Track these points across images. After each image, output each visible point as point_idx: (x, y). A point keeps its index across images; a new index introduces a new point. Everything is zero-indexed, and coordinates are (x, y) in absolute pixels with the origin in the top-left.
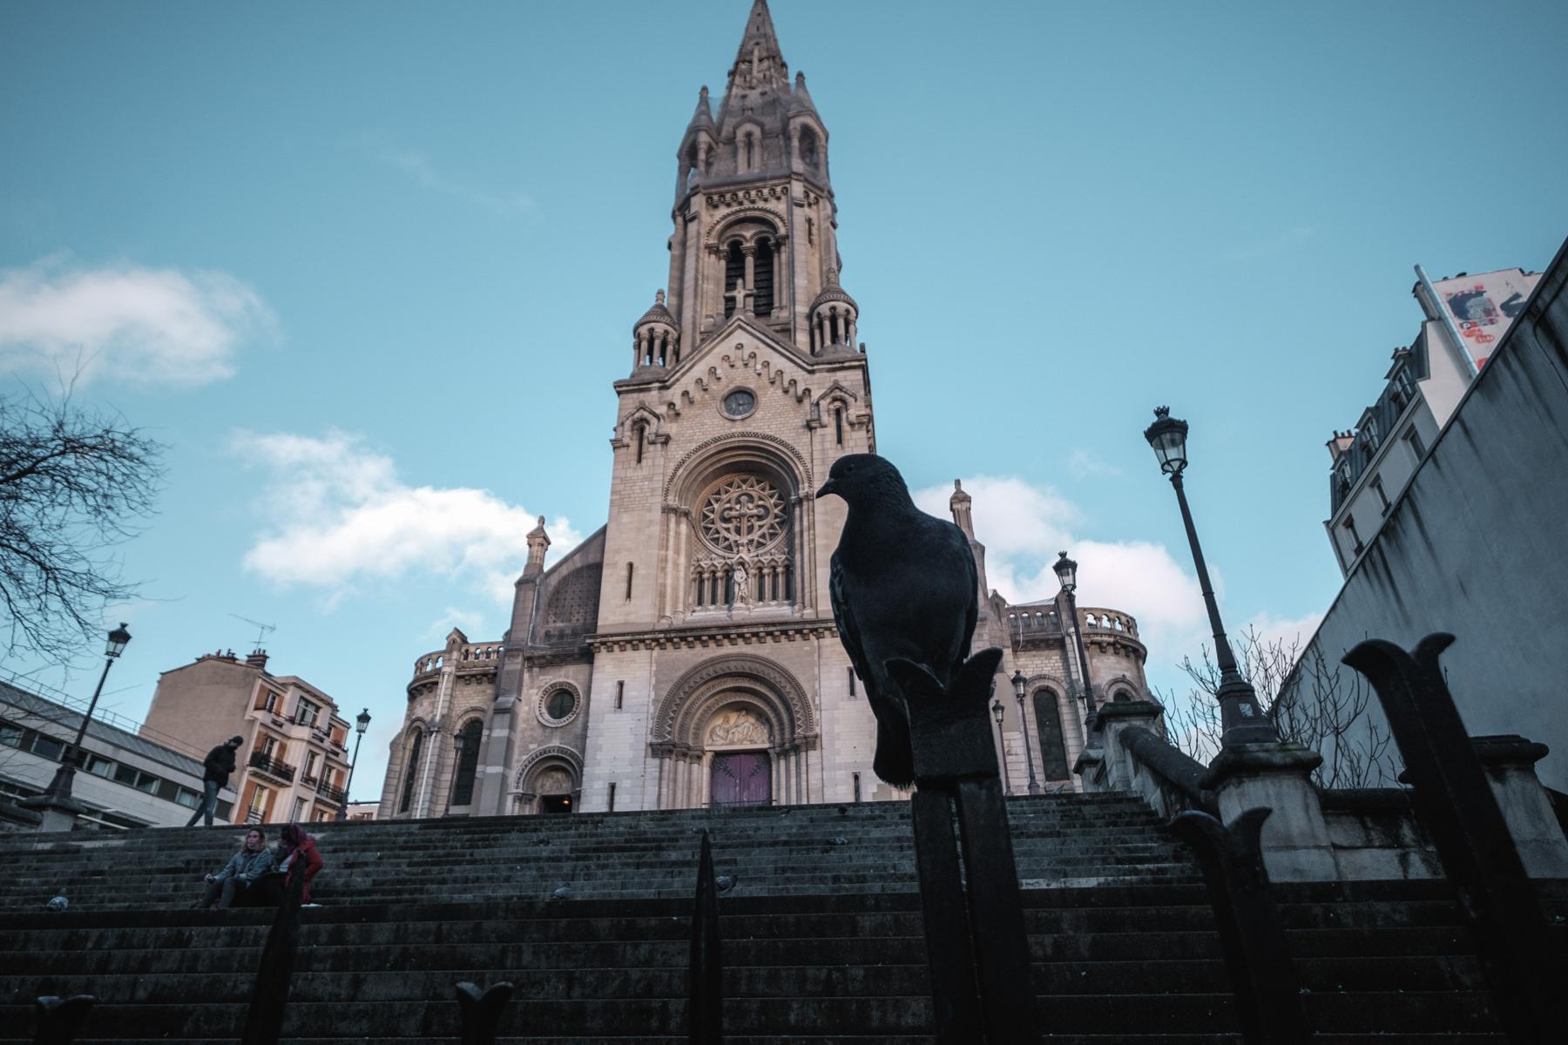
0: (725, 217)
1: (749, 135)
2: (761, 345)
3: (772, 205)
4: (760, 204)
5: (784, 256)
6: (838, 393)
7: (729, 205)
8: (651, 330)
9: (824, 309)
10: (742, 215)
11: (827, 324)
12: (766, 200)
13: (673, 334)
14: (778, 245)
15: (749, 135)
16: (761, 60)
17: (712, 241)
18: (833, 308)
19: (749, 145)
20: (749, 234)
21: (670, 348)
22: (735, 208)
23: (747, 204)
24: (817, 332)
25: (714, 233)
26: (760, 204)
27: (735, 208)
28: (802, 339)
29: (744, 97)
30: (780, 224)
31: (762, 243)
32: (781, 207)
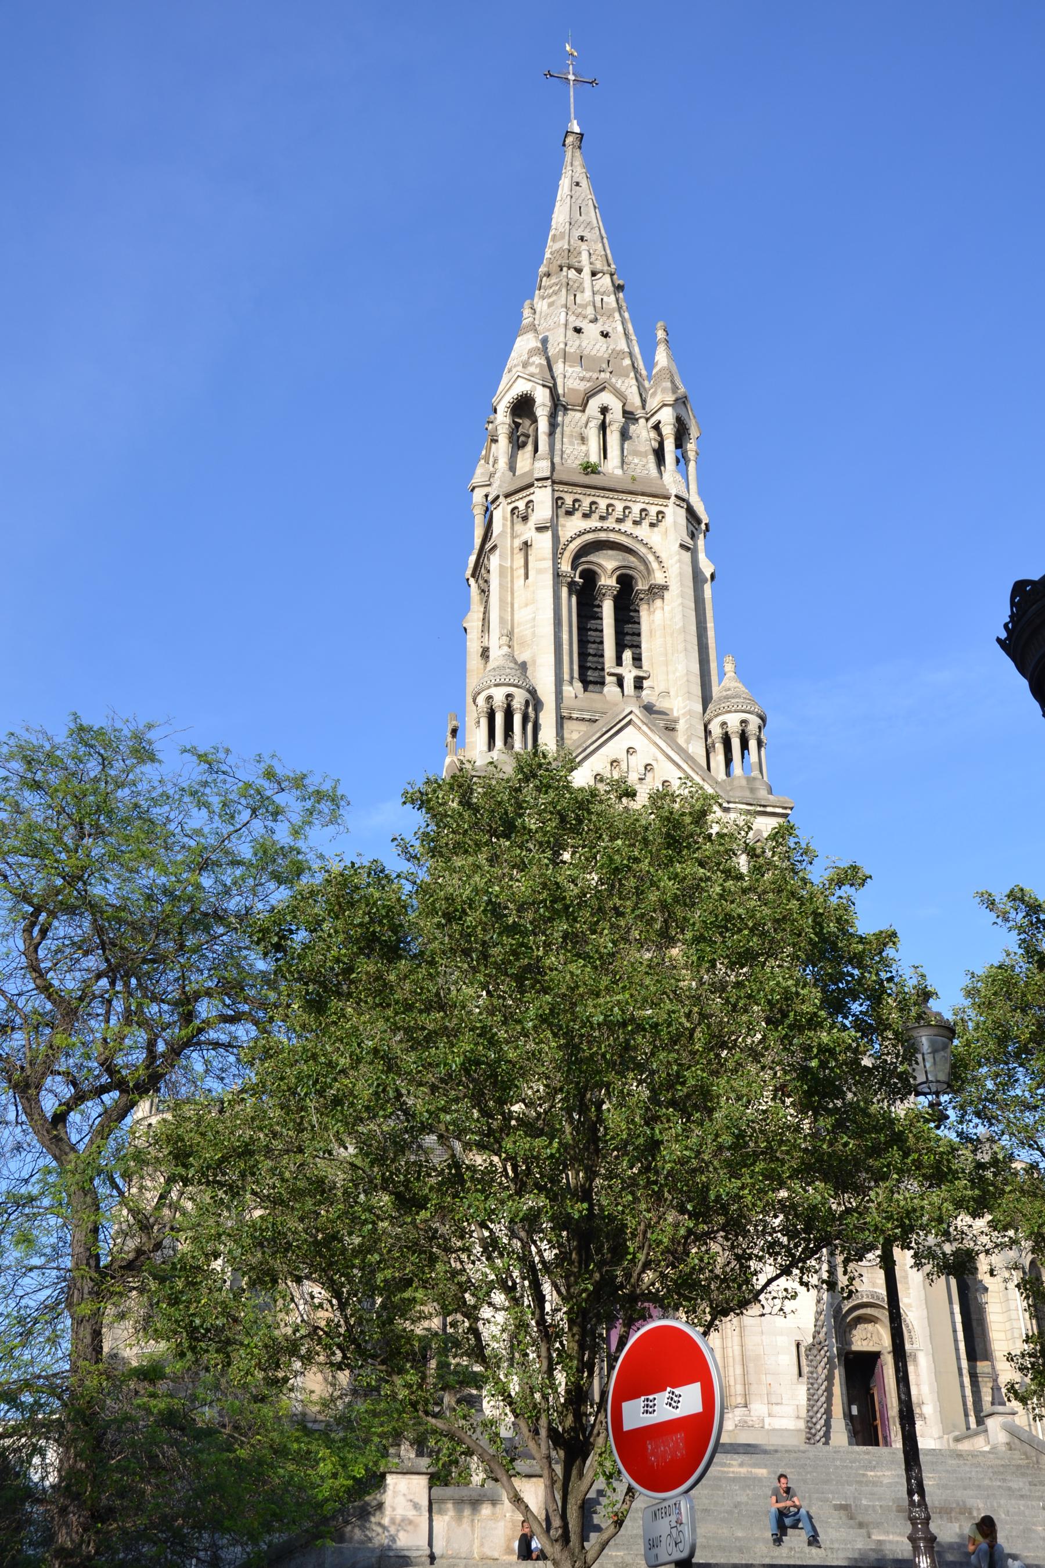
0: (580, 534)
1: (604, 410)
2: (661, 757)
3: (642, 531)
5: (658, 614)
7: (586, 516)
8: (509, 696)
10: (603, 536)
11: (736, 743)
13: (520, 698)
15: (604, 410)
16: (594, 274)
21: (530, 726)
22: (594, 523)
23: (610, 523)
24: (719, 747)
26: (627, 526)
28: (697, 750)
30: (655, 565)
31: (626, 582)
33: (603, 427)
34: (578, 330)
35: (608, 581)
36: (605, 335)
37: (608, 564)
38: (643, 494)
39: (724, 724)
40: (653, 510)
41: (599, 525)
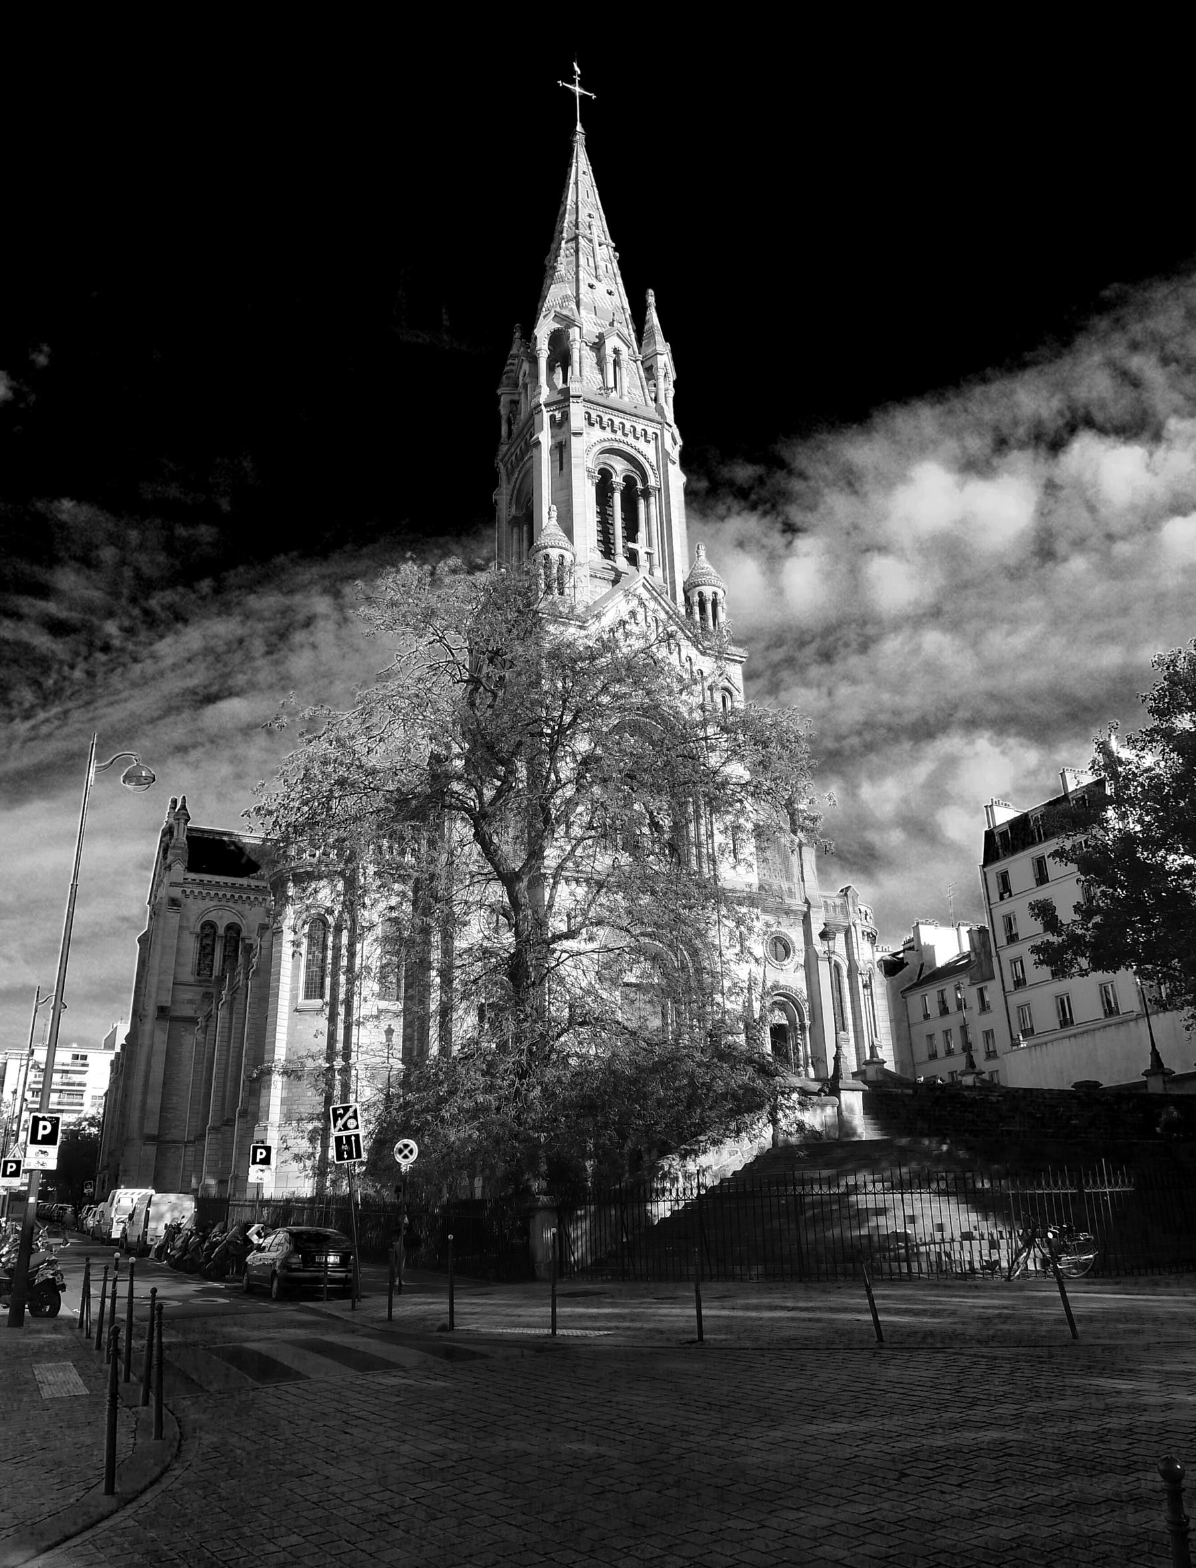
4: (630, 439)
6: (727, 684)
7: (603, 428)
9: (708, 592)
12: (637, 438)
14: (646, 494)
16: (600, 245)
17: (590, 465)
18: (715, 593)
19: (616, 363)
20: (620, 468)
25: (591, 455)
26: (630, 439)
27: (608, 434)
29: (591, 286)
32: (649, 450)
33: (616, 363)
34: (591, 286)
35: (618, 480)
36: (610, 293)
37: (620, 468)
38: (644, 418)
39: (701, 594)
40: (650, 431)
41: (613, 436)
